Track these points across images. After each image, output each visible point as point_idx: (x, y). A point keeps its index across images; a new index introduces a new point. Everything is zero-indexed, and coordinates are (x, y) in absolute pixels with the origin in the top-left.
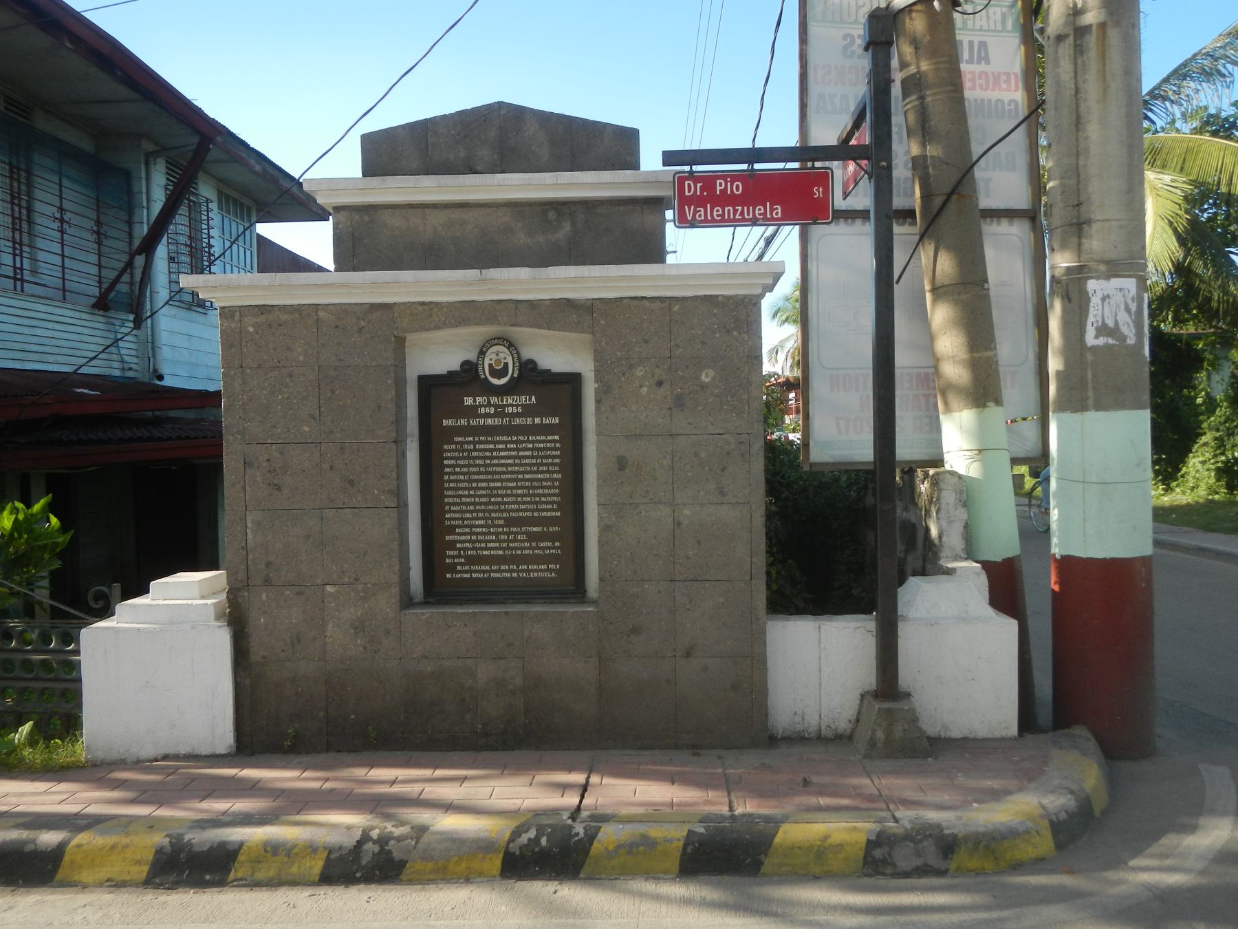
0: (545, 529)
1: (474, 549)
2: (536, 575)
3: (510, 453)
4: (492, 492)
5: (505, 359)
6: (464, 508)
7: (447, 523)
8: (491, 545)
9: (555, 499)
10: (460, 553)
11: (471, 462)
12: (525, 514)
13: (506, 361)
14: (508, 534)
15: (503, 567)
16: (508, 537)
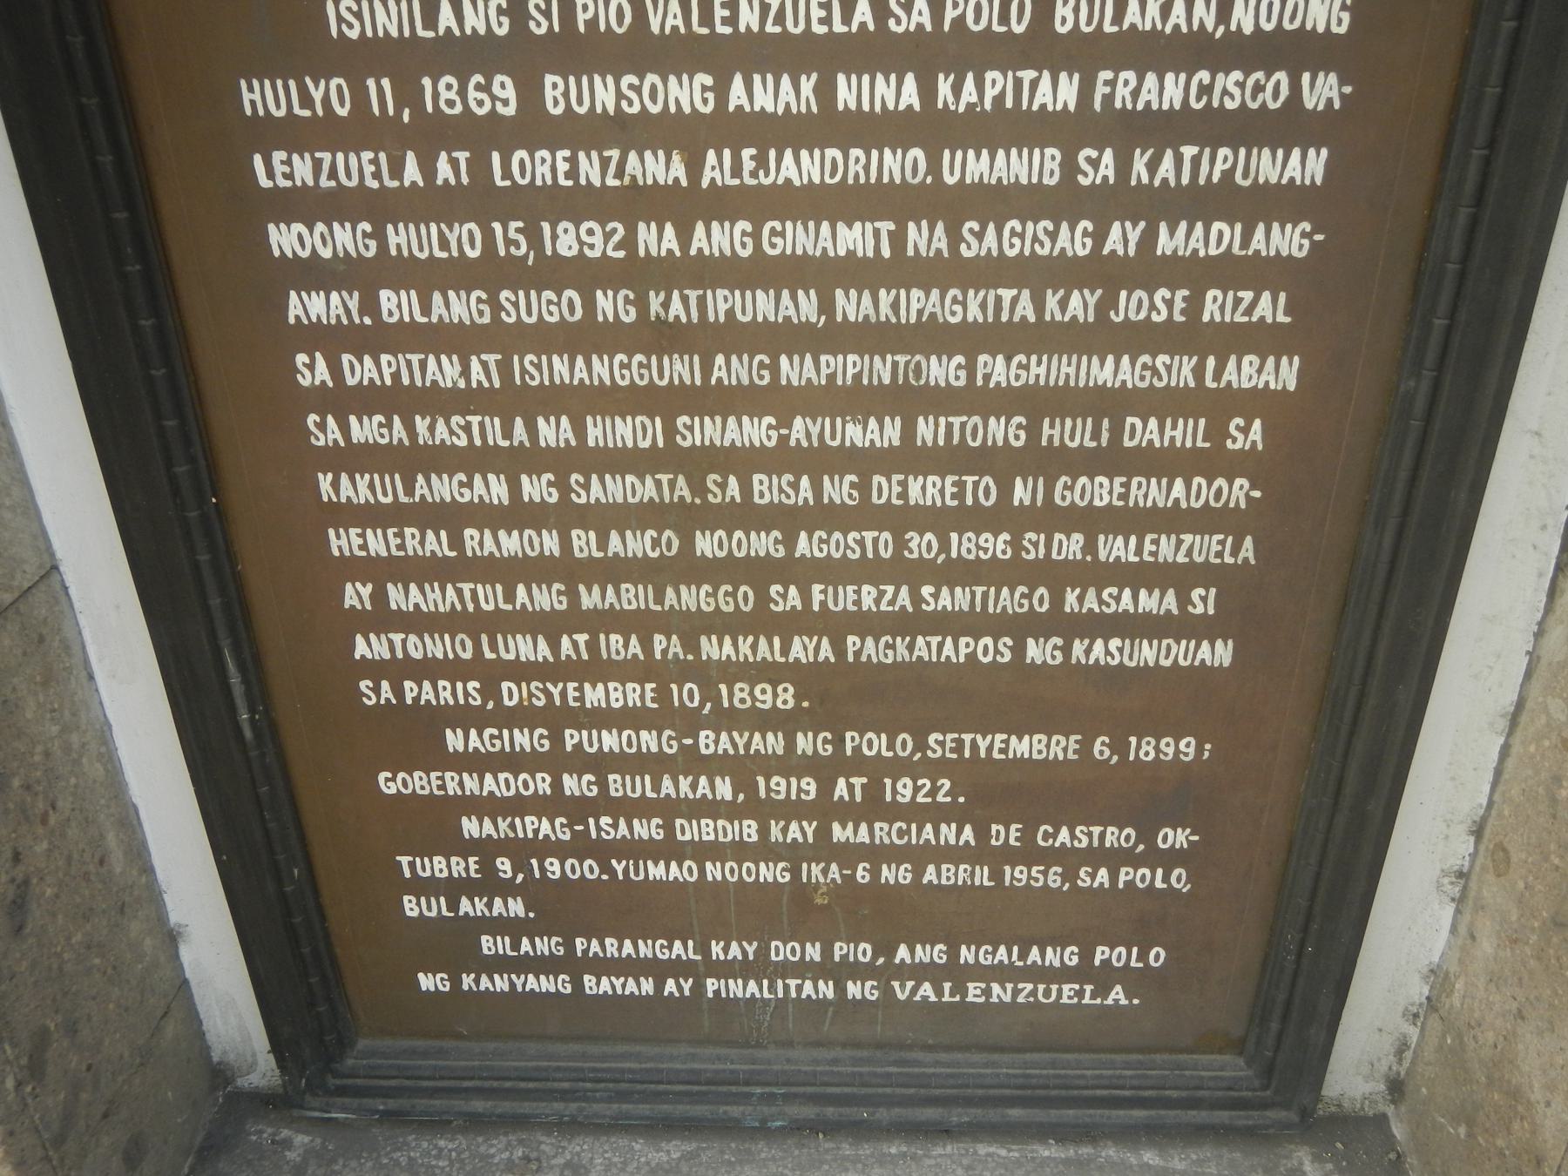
0: (1100, 748)
1: (582, 847)
2: (1000, 993)
3: (857, 164)
4: (699, 488)
6: (489, 598)
7: (374, 694)
8: (707, 830)
9: (1206, 547)
10: (487, 867)
11: (510, 235)
12: (955, 650)
14: (825, 770)
15: (781, 951)
16: (826, 788)
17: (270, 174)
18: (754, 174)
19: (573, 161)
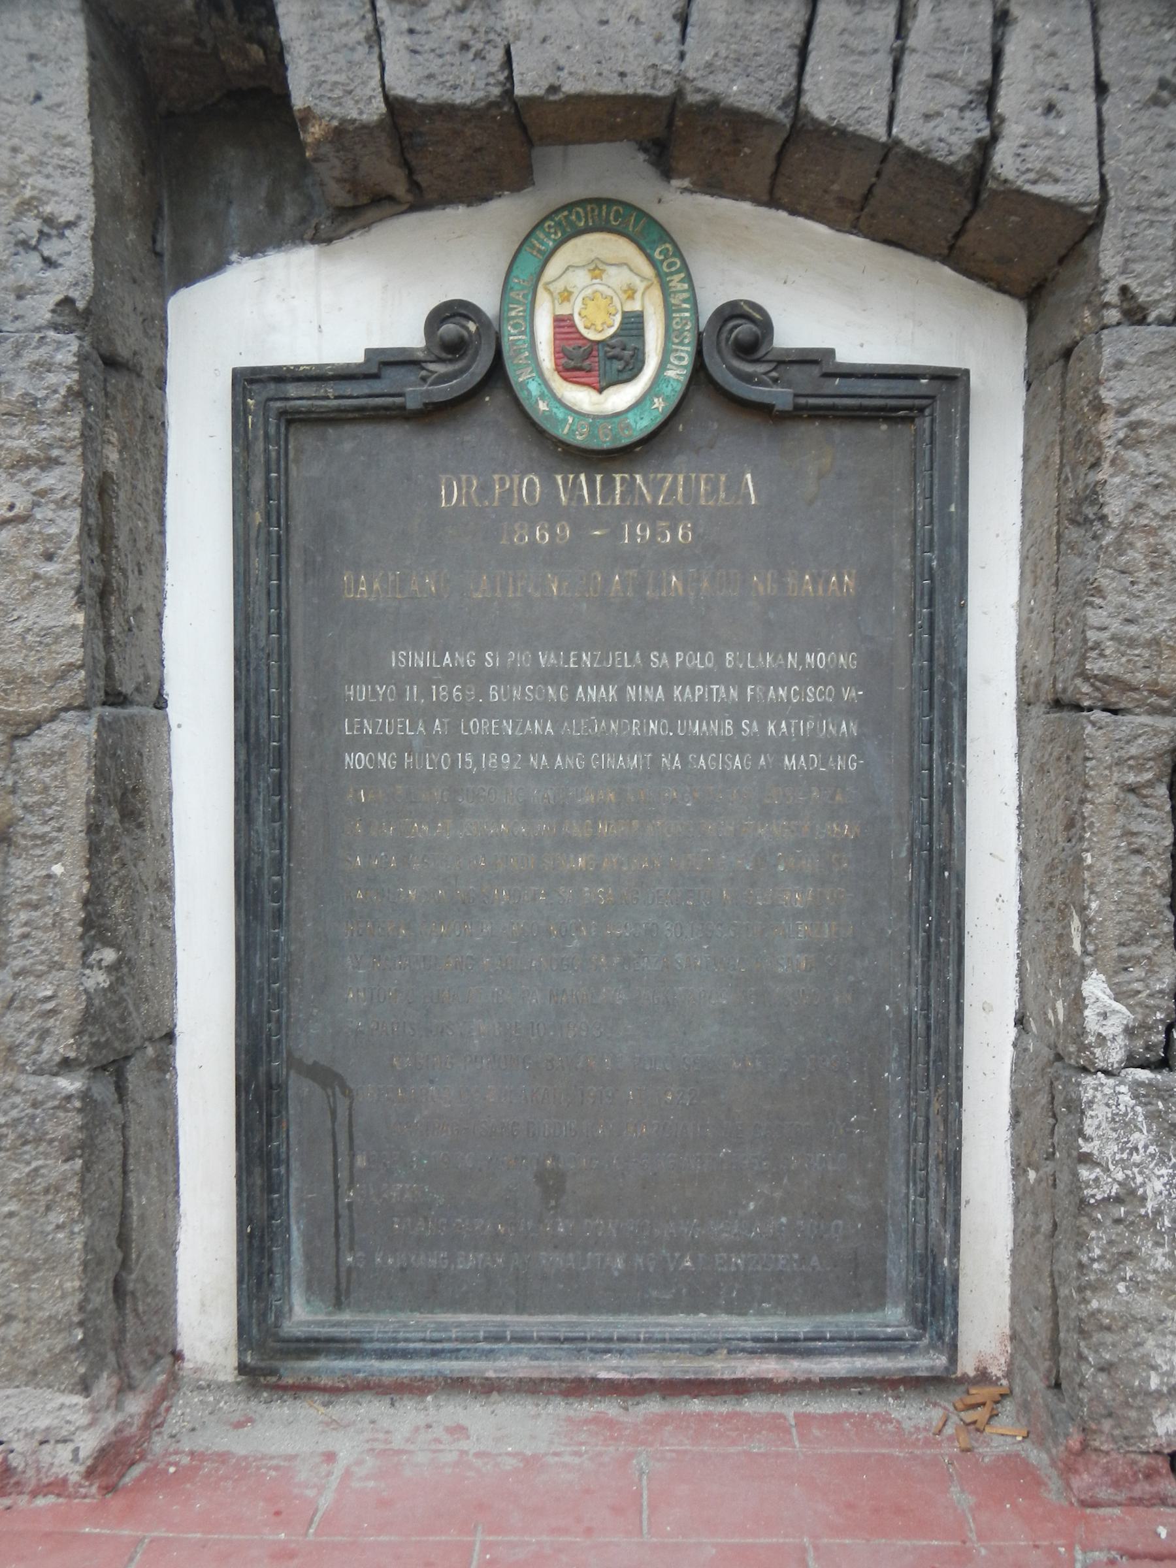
5: (631, 292)
13: (635, 306)
17: (351, 729)
18: (586, 730)
19: (499, 723)
